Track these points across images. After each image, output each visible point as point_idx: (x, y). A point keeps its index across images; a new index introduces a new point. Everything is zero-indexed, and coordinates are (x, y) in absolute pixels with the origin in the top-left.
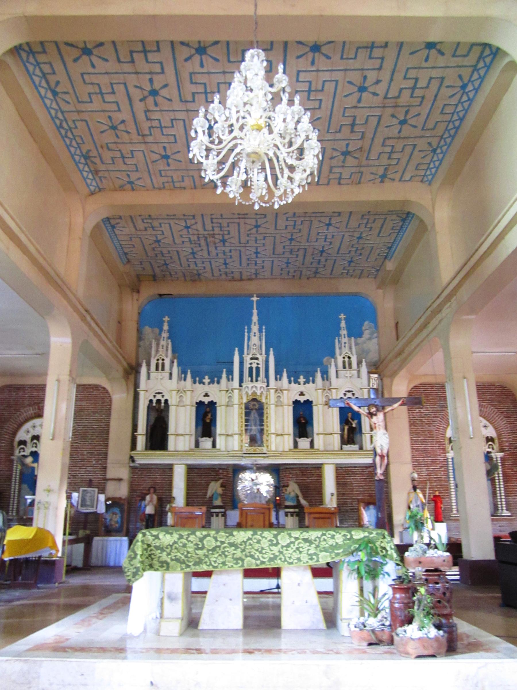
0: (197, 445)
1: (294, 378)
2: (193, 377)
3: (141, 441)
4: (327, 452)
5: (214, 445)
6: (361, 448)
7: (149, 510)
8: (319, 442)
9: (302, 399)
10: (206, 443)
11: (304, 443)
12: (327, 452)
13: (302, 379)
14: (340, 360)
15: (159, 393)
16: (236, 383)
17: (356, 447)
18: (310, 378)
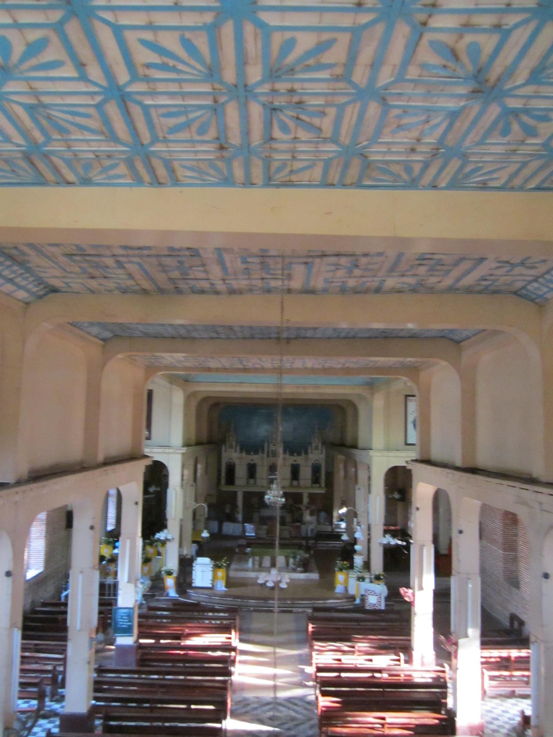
0: (248, 483)
1: (292, 454)
2: (246, 451)
3: (223, 481)
4: (306, 487)
5: (255, 483)
6: (320, 487)
7: (227, 511)
8: (302, 483)
9: (295, 463)
10: (252, 481)
11: (295, 483)
12: (306, 487)
13: (295, 454)
14: (314, 445)
15: (231, 459)
16: (265, 456)
17: (318, 485)
18: (299, 454)
